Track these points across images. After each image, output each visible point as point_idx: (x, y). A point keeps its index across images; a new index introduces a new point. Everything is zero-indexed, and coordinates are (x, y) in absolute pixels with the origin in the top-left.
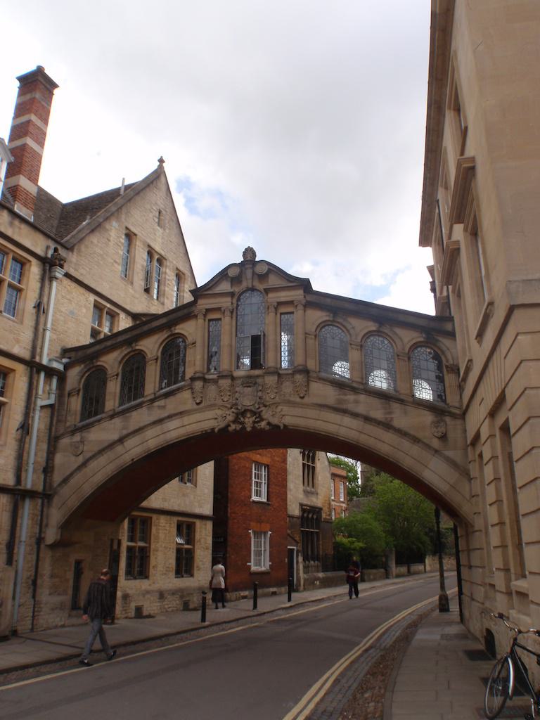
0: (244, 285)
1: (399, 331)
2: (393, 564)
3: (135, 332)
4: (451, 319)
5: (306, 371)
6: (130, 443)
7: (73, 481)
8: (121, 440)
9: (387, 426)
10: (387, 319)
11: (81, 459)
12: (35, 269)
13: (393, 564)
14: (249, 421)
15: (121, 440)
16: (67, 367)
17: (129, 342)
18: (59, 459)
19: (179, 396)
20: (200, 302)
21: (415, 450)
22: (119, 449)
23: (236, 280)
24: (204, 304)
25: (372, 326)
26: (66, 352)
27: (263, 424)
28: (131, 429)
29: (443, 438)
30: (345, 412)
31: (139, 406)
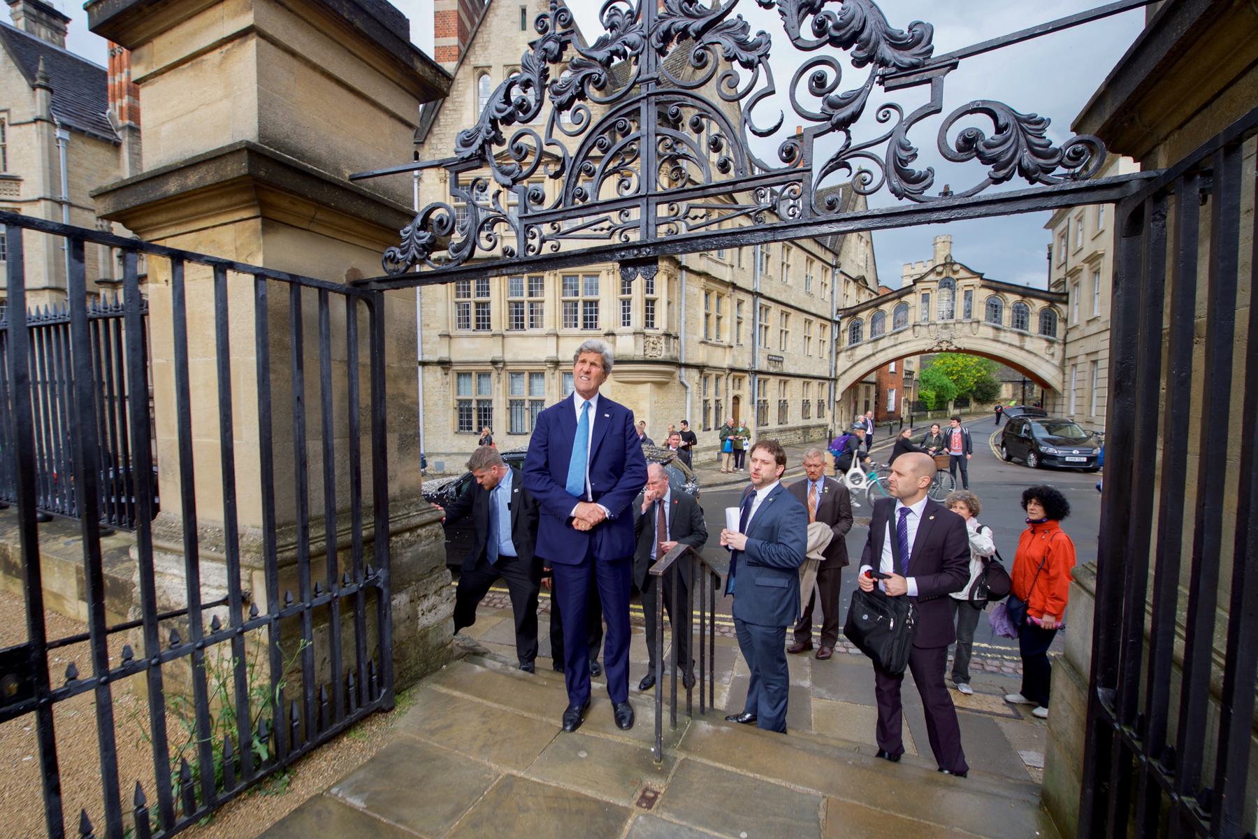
0: (944, 275)
1: (1033, 300)
2: (951, 406)
3: (879, 301)
4: (1067, 294)
5: (978, 322)
6: (877, 355)
7: (848, 373)
8: (873, 354)
9: (1021, 348)
10: (1027, 293)
11: (850, 364)
12: (830, 272)
13: (951, 406)
14: (944, 346)
15: (873, 354)
16: (841, 318)
17: (876, 306)
18: (839, 363)
19: (905, 333)
20: (918, 285)
21: (1035, 360)
22: (873, 358)
23: (941, 273)
24: (919, 286)
25: (1018, 298)
26: (838, 310)
27: (953, 348)
28: (879, 348)
29: (1053, 355)
30: (998, 341)
31: (884, 337)
